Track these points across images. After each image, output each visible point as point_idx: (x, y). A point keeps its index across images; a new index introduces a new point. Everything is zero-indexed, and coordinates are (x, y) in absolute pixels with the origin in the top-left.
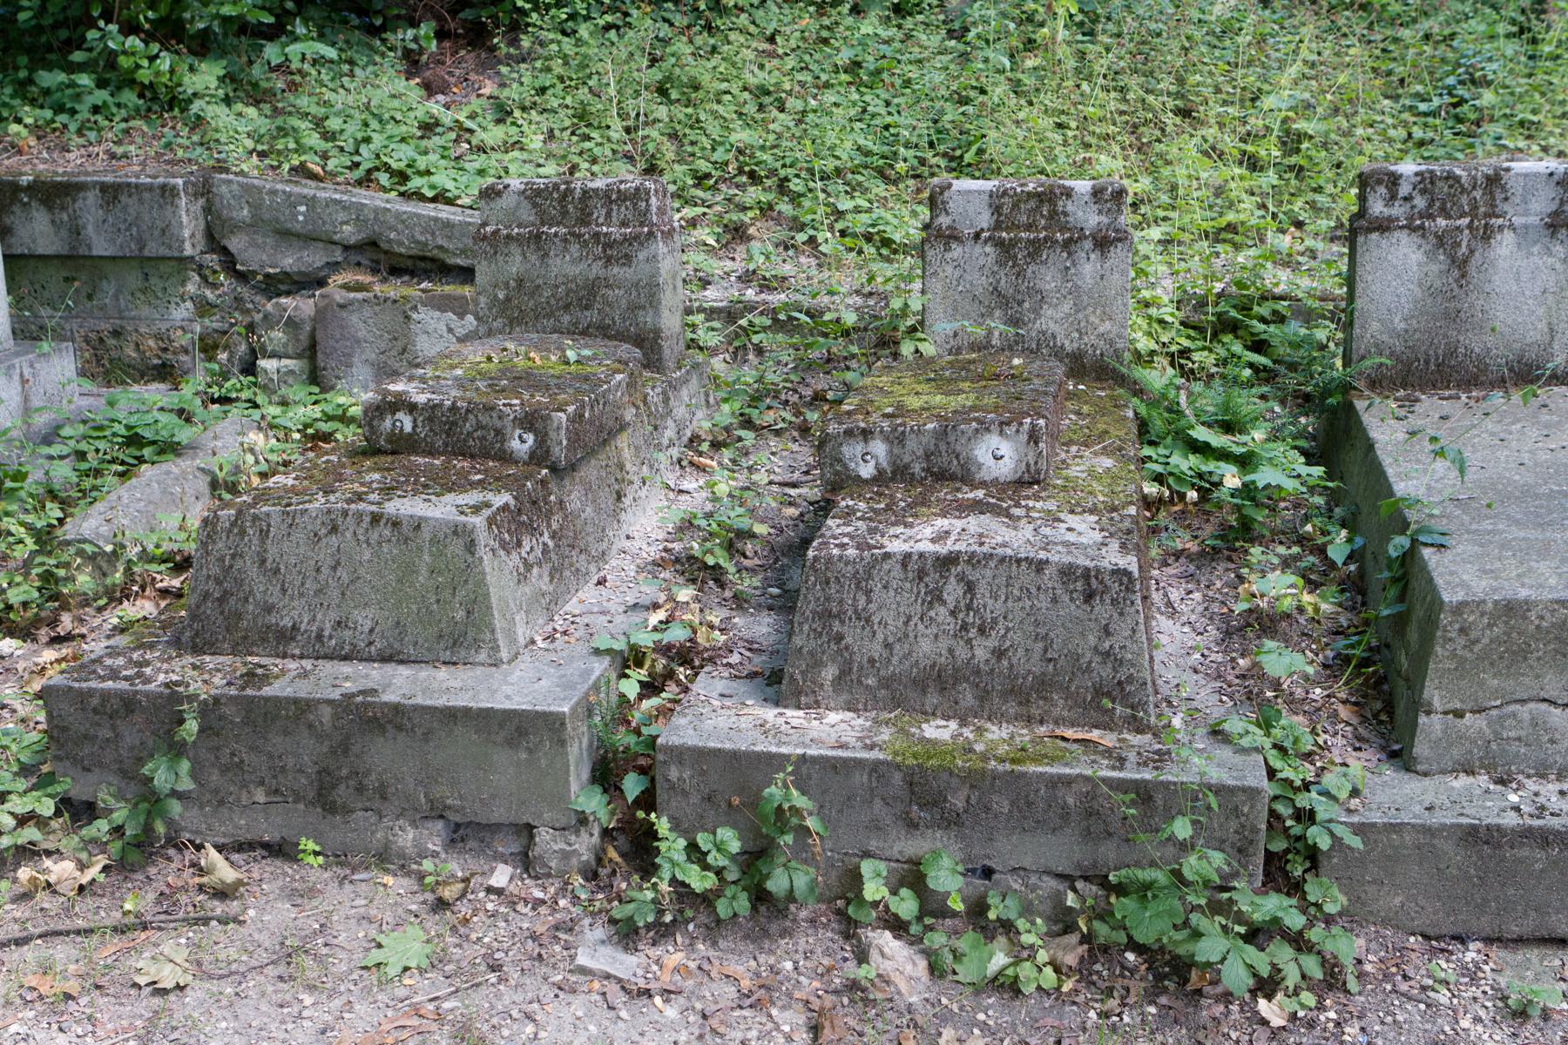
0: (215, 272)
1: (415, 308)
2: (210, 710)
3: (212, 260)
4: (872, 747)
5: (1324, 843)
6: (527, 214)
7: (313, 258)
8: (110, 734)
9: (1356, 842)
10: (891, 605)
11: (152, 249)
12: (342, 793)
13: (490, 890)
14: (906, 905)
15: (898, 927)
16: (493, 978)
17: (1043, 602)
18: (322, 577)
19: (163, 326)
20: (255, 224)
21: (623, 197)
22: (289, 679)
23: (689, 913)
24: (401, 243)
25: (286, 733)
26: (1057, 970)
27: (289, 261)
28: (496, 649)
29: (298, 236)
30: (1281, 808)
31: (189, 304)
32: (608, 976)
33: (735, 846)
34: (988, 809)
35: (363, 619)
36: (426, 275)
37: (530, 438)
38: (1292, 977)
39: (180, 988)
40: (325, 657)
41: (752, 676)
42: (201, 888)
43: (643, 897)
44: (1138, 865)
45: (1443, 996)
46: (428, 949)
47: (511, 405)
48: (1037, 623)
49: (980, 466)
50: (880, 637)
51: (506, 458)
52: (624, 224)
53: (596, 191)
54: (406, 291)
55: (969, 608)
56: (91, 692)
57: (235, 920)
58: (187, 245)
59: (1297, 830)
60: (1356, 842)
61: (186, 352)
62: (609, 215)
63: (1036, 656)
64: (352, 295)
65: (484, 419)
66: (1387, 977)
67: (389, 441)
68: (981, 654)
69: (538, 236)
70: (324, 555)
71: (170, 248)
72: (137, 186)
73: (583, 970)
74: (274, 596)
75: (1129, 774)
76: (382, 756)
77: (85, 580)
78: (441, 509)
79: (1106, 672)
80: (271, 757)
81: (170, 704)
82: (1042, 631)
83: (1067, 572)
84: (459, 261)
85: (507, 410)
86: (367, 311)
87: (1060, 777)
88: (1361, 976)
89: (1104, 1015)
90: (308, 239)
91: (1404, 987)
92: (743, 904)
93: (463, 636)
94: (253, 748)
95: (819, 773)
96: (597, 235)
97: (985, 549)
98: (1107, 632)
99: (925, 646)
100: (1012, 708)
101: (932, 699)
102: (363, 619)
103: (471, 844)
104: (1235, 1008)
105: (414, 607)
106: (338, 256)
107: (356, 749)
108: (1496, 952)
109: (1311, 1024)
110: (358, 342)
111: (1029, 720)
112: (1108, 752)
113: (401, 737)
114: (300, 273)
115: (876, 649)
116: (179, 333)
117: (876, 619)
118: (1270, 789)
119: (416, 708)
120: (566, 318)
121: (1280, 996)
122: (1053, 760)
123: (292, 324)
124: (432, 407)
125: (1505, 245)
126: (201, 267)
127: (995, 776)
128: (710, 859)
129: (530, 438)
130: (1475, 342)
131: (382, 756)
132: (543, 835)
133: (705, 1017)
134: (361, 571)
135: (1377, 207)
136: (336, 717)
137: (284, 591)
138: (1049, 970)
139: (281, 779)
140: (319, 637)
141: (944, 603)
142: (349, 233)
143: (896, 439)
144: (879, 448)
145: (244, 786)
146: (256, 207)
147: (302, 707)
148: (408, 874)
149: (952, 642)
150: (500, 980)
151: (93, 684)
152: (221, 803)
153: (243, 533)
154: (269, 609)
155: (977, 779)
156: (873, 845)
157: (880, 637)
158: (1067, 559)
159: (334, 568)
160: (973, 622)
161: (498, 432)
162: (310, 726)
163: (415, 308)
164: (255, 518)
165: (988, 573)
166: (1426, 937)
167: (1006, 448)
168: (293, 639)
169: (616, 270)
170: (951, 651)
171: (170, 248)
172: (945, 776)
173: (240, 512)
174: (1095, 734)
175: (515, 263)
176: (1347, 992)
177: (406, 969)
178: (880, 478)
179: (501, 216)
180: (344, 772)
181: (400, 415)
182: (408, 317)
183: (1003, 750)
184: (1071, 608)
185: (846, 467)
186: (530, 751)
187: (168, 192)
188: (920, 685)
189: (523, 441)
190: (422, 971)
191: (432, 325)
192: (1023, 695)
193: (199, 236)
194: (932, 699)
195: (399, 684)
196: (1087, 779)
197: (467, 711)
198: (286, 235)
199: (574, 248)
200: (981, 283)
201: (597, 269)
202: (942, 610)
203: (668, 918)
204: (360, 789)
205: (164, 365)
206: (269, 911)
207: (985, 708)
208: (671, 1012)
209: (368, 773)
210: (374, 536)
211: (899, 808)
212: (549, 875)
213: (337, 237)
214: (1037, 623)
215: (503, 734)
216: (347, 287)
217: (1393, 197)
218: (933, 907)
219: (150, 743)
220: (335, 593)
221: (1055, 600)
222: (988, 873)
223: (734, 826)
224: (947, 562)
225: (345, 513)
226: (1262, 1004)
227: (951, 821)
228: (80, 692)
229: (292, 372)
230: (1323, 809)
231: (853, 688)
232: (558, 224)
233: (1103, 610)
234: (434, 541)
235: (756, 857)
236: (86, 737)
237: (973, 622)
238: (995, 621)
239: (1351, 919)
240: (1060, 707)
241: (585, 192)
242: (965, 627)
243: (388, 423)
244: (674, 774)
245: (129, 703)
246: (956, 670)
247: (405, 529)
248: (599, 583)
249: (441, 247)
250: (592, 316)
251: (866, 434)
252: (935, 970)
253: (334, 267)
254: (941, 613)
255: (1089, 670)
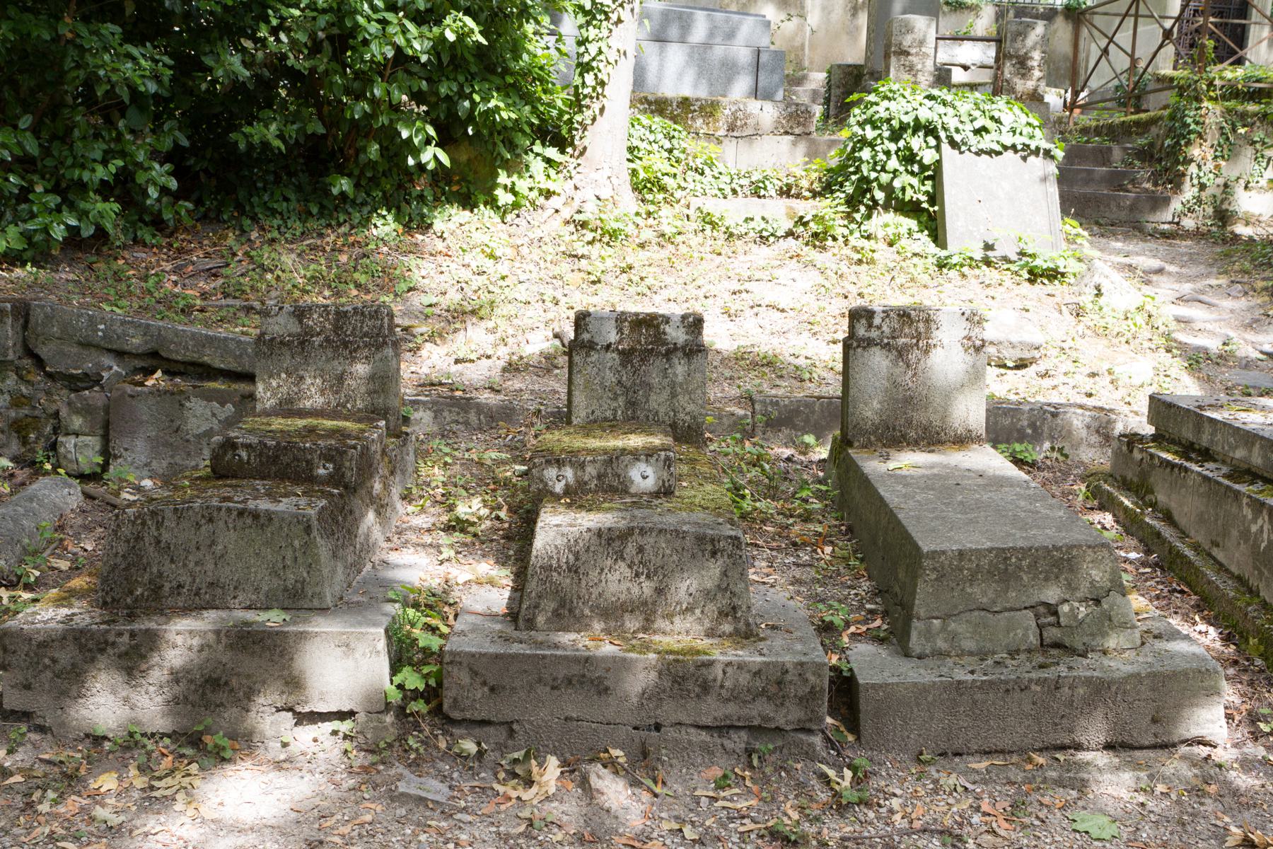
1: (188, 399)
3: (27, 362)
29: (97, 347)
49: (632, 482)
137: (172, 561)
153: (144, 524)
167: (649, 471)
178: (568, 491)
182: (182, 405)
185: (546, 484)
200: (611, 378)
217: (870, 326)
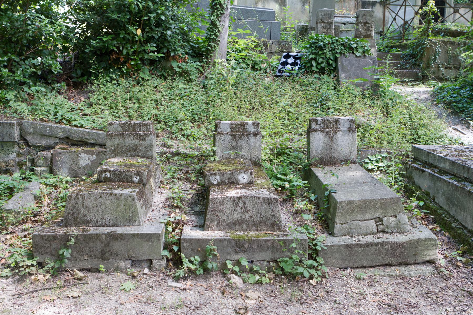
0: (22, 145)
1: (80, 154)
2: (77, 237)
3: (22, 142)
4: (227, 236)
5: (320, 249)
6: (120, 129)
7: (51, 141)
8: (49, 245)
9: (326, 248)
10: (227, 208)
11: (6, 139)
12: (107, 255)
13: (143, 274)
14: (237, 269)
15: (236, 273)
16: (151, 289)
17: (260, 205)
18: (98, 208)
19: (7, 160)
20: (35, 133)
21: (144, 125)
22: (92, 231)
23: (190, 274)
24: (75, 137)
25: (94, 242)
26: (269, 279)
27: (44, 142)
28: (140, 222)
29: (47, 136)
30: (310, 244)
31: (15, 154)
32: (176, 287)
33: (199, 260)
34: (252, 248)
35: (108, 217)
36: (81, 145)
37: (138, 178)
38: (316, 276)
39: (79, 296)
40: (98, 226)
41: (195, 226)
42: (74, 279)
43: (180, 273)
44: (283, 257)
45: (344, 277)
46: (134, 285)
47: (134, 171)
48: (259, 210)
49: (240, 181)
50: (226, 214)
51: (132, 182)
52: (144, 131)
53: (137, 124)
54: (77, 149)
55: (244, 207)
56: (45, 236)
57: (87, 283)
58: (16, 138)
59: (314, 248)
60: (326, 248)
61: (14, 166)
62: (140, 129)
63: (259, 217)
64: (63, 150)
65: (127, 174)
66: (333, 275)
67: (104, 179)
68: (247, 217)
69: (123, 134)
70: (98, 203)
71: (11, 139)
72: (3, 123)
73: (170, 286)
74: (86, 213)
75: (281, 238)
76: (117, 246)
77: (11, 218)
78: (126, 192)
79: (273, 219)
80: (90, 248)
81: (66, 238)
82: (260, 211)
83: (264, 199)
84: (91, 142)
85: (133, 171)
86: (67, 155)
87: (267, 240)
88: (329, 275)
89: (280, 286)
90: (50, 136)
91: (337, 277)
92: (202, 271)
93: (131, 220)
94: (85, 246)
95: (218, 242)
96: (137, 134)
97: (247, 195)
98: (273, 211)
99: (236, 216)
100: (254, 228)
101: (237, 227)
102: (108, 217)
103: (137, 265)
104: (305, 283)
105: (120, 214)
106: (58, 141)
107: (111, 245)
108: (353, 269)
109: (321, 284)
110: (64, 162)
111: (258, 230)
112: (275, 235)
113: (122, 241)
114: (47, 145)
115: (225, 217)
116: (12, 161)
117: (225, 211)
118: (309, 241)
119: (126, 234)
120: (129, 154)
121: (314, 279)
122: (265, 237)
123: (45, 158)
124: (115, 171)
125: (340, 134)
126: (19, 144)
127: (254, 240)
128: (194, 262)
129: (138, 178)
130: (335, 155)
131: (117, 246)
132: (155, 262)
133: (199, 292)
134: (107, 206)
135: (314, 126)
136: (106, 237)
137: (88, 211)
138: (268, 279)
139: (92, 253)
140: (97, 222)
141: (239, 206)
142: (61, 135)
143: (222, 175)
144: (218, 177)
145: (82, 255)
146: (35, 129)
147: (98, 236)
148: (123, 273)
149: (241, 215)
150: (153, 289)
151: (46, 234)
152: (76, 260)
153: (78, 198)
154: (85, 216)
155: (250, 241)
156: (228, 257)
157: (226, 214)
158: (264, 196)
159: (101, 206)
160: (245, 210)
161: (130, 176)
162: (100, 240)
163: (80, 154)
164: (81, 195)
165: (248, 200)
166: (340, 268)
167: (245, 176)
168: (90, 222)
169: (142, 142)
170: (241, 217)
171: (11, 139)
172: (243, 241)
173: (77, 194)
174: (272, 232)
175: (117, 141)
176: (326, 278)
177: (131, 289)
178: (218, 184)
179: (113, 129)
180: (108, 250)
181: (107, 173)
182: (78, 156)
183: (254, 235)
184: (265, 206)
185: (211, 182)
186: (152, 242)
187: (11, 125)
188: (235, 224)
189: (136, 178)
190: (134, 289)
191: (85, 158)
192: (256, 225)
193: (19, 137)
194: (237, 227)
195: (119, 230)
196: (272, 240)
197: (138, 234)
198: (43, 135)
199: (132, 137)
200: (228, 144)
201: (137, 142)
202: (239, 208)
203: (186, 275)
204: (111, 254)
205: (7, 170)
206: (93, 281)
207: (248, 228)
208: (191, 292)
209: (113, 250)
210: (111, 198)
211: (234, 249)
212: (156, 270)
213: (58, 136)
214: (259, 210)
215: (146, 239)
216: (60, 148)
217: (317, 124)
218: (243, 270)
219: (59, 247)
220: (101, 212)
221: (262, 205)
222: (252, 262)
223: (198, 255)
224: (239, 198)
225: (103, 193)
226: (311, 281)
227: (245, 251)
228: (42, 236)
229: (44, 171)
230: (319, 244)
231: (220, 226)
232: (128, 131)
233: (272, 206)
234: (125, 198)
235: (202, 263)
236: (43, 246)
237: (245, 210)
238: (250, 210)
239: (326, 265)
240: (264, 228)
241: (134, 124)
242: (244, 211)
243: (104, 175)
244: (185, 245)
245: (55, 237)
246: (242, 221)
247: (118, 196)
248: (153, 211)
249: (86, 138)
250: (136, 153)
251: (215, 174)
252: (244, 281)
253: (56, 144)
254: (239, 209)
255: (269, 219)
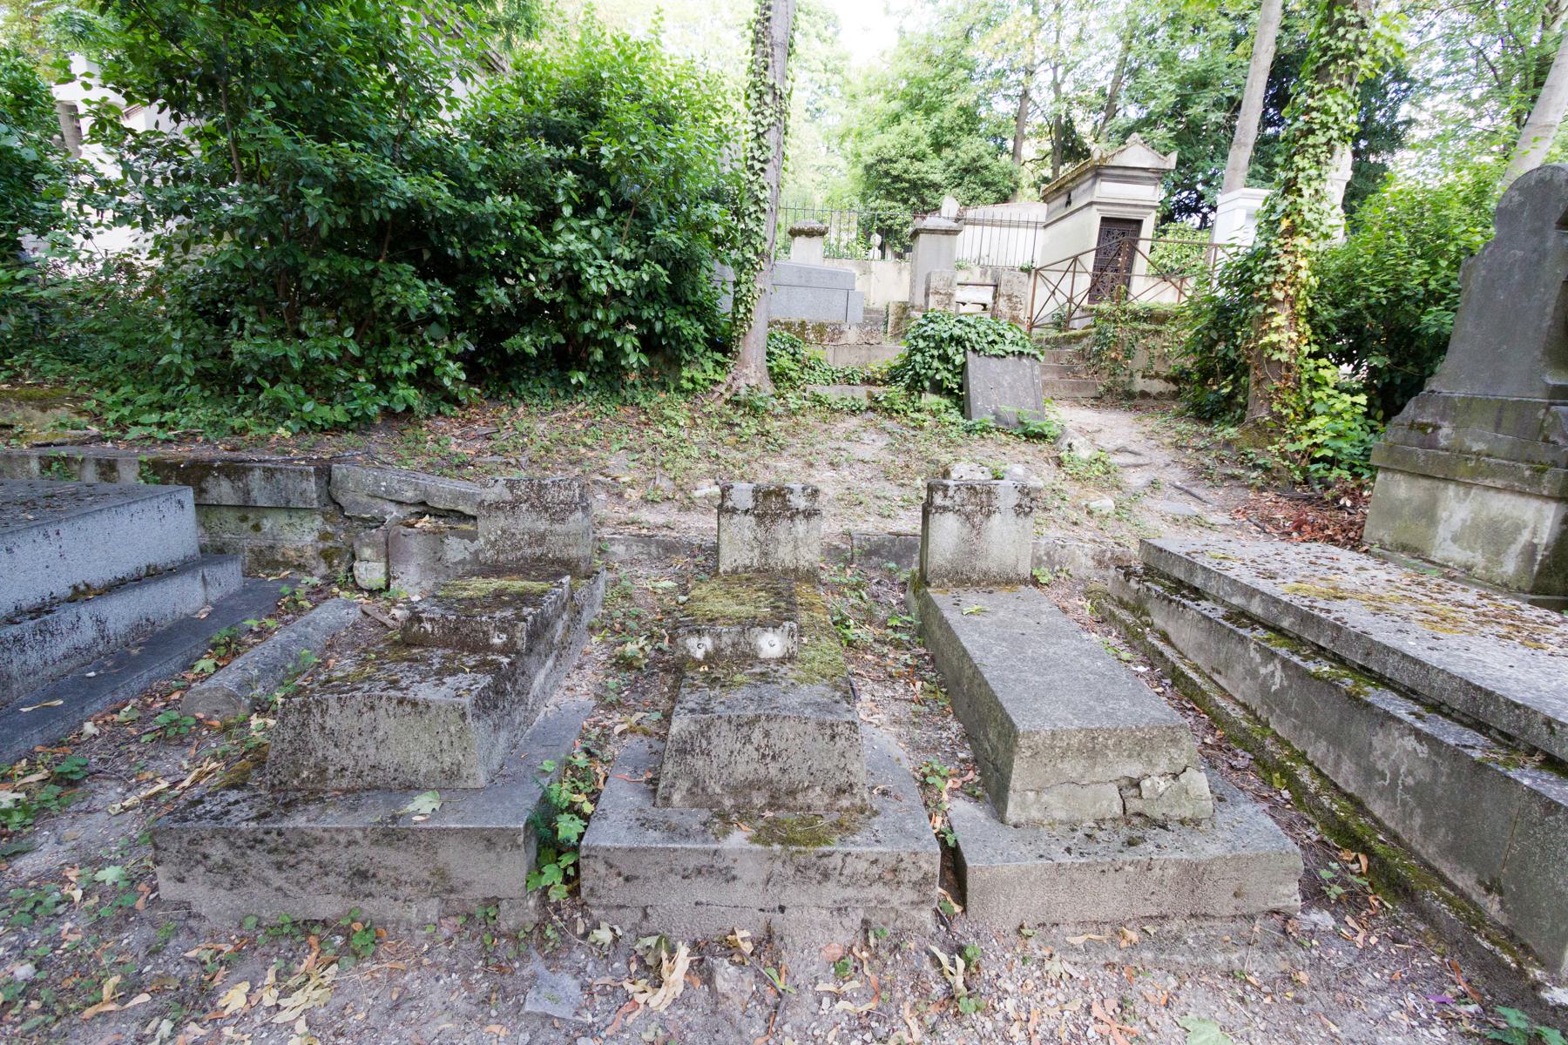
3: (330, 508)
17: (808, 739)
37: (504, 636)
125: (996, 519)
129: (504, 636)
130: (981, 565)
135: (938, 499)
153: (309, 712)
184: (822, 743)
200: (748, 535)
221: (814, 740)
